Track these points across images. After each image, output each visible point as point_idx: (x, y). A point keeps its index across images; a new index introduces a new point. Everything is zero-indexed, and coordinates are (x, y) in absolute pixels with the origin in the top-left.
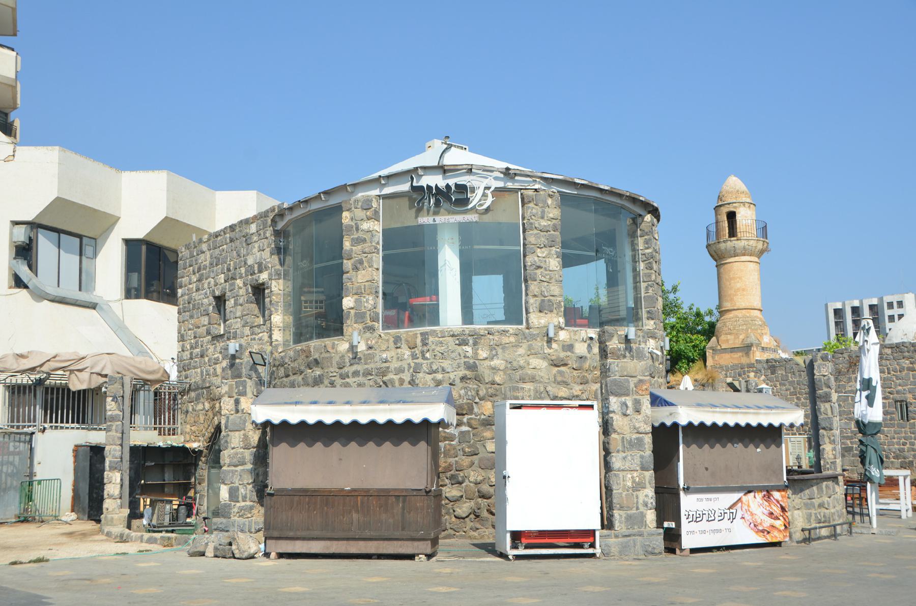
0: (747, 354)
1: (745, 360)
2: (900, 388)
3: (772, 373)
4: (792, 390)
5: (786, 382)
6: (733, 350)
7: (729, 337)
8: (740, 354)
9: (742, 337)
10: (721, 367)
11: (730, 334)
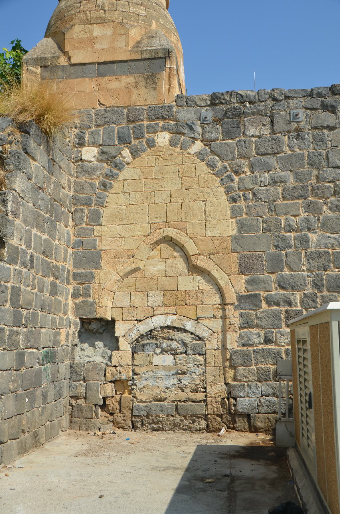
0: (152, 80)
3: (228, 134)
4: (291, 182)
5: (272, 160)
6: (106, 67)
7: (96, 30)
8: (130, 79)
9: (135, 34)
11: (102, 22)
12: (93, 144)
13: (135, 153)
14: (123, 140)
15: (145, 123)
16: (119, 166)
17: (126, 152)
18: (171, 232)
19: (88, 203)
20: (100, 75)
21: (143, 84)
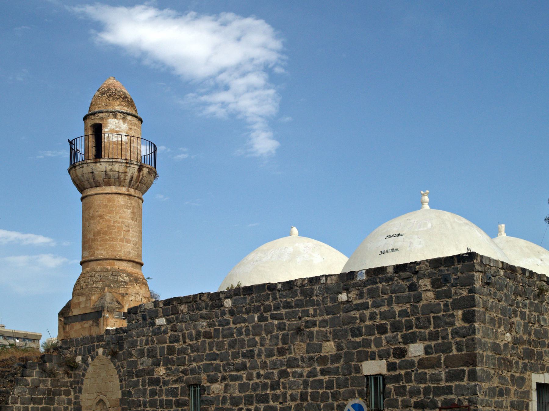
1: (95, 331)
2: (194, 365)
10: (72, 341)
12: (79, 355)
13: (92, 359)
14: (89, 353)
15: (96, 344)
16: (88, 365)
17: (90, 358)
18: (102, 397)
19: (78, 383)
20: (82, 320)
21: (95, 324)
